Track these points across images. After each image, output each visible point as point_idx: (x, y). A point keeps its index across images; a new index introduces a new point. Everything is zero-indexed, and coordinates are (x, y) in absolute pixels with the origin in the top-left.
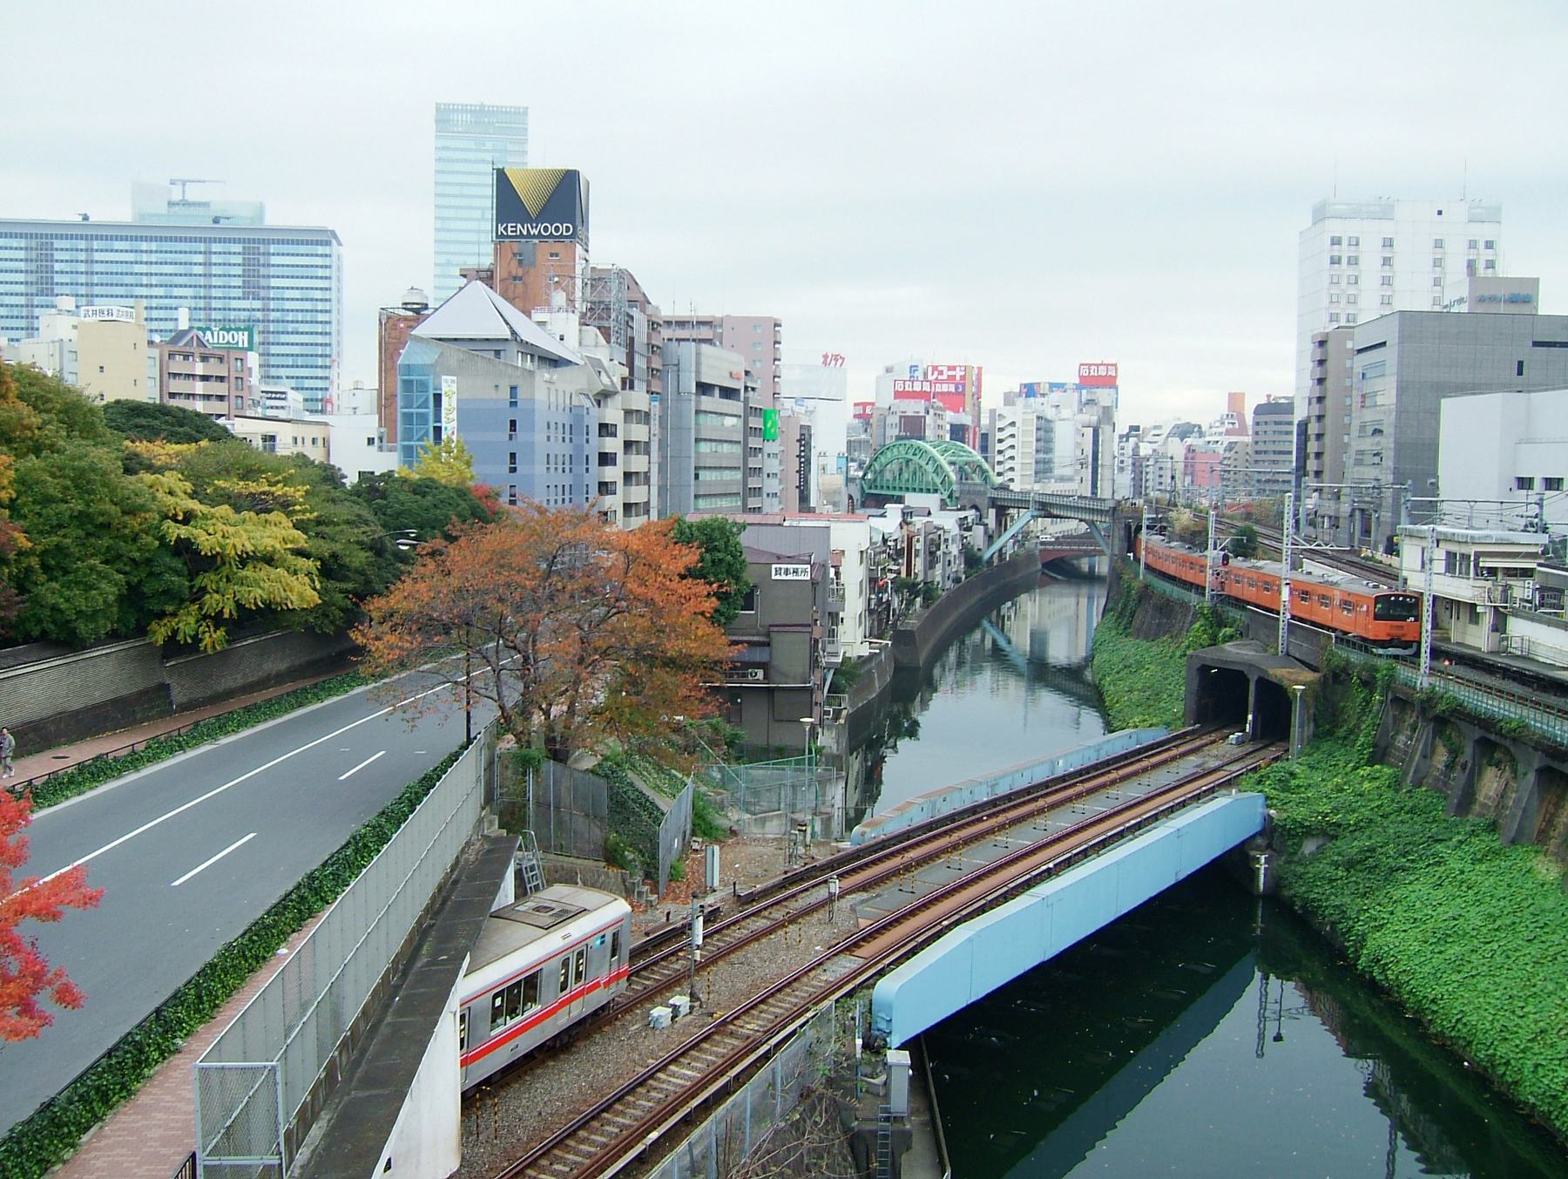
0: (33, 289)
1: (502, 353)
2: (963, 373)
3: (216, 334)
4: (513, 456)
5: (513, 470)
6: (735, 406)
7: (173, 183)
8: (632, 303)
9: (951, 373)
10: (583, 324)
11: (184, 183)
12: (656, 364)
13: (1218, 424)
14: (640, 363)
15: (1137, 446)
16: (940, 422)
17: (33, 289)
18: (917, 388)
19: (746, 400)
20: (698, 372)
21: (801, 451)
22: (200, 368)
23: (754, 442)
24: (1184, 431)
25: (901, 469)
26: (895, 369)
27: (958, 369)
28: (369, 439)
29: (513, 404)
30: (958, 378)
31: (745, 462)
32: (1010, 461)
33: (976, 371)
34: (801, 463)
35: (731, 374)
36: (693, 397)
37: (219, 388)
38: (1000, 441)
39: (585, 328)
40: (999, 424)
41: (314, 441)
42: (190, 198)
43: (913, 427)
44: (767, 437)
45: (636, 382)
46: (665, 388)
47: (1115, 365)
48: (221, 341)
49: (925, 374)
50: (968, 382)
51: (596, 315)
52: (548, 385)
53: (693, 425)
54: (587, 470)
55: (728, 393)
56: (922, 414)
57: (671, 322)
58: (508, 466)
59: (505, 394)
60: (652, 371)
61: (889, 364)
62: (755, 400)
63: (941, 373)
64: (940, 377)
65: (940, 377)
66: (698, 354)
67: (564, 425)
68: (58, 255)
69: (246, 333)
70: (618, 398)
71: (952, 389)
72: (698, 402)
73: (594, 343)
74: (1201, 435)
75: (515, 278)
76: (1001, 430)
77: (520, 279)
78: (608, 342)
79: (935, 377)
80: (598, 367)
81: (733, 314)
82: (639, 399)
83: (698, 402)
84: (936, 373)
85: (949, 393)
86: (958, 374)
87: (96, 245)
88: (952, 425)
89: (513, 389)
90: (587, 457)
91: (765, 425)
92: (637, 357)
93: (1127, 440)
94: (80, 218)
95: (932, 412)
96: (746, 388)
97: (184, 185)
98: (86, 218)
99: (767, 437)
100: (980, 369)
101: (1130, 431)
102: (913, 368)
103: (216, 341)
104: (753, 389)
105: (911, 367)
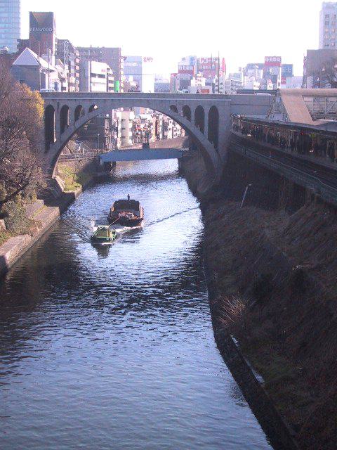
6: (104, 80)
43: (185, 84)
55: (101, 76)
62: (111, 79)
95: (194, 78)
100: (223, 59)
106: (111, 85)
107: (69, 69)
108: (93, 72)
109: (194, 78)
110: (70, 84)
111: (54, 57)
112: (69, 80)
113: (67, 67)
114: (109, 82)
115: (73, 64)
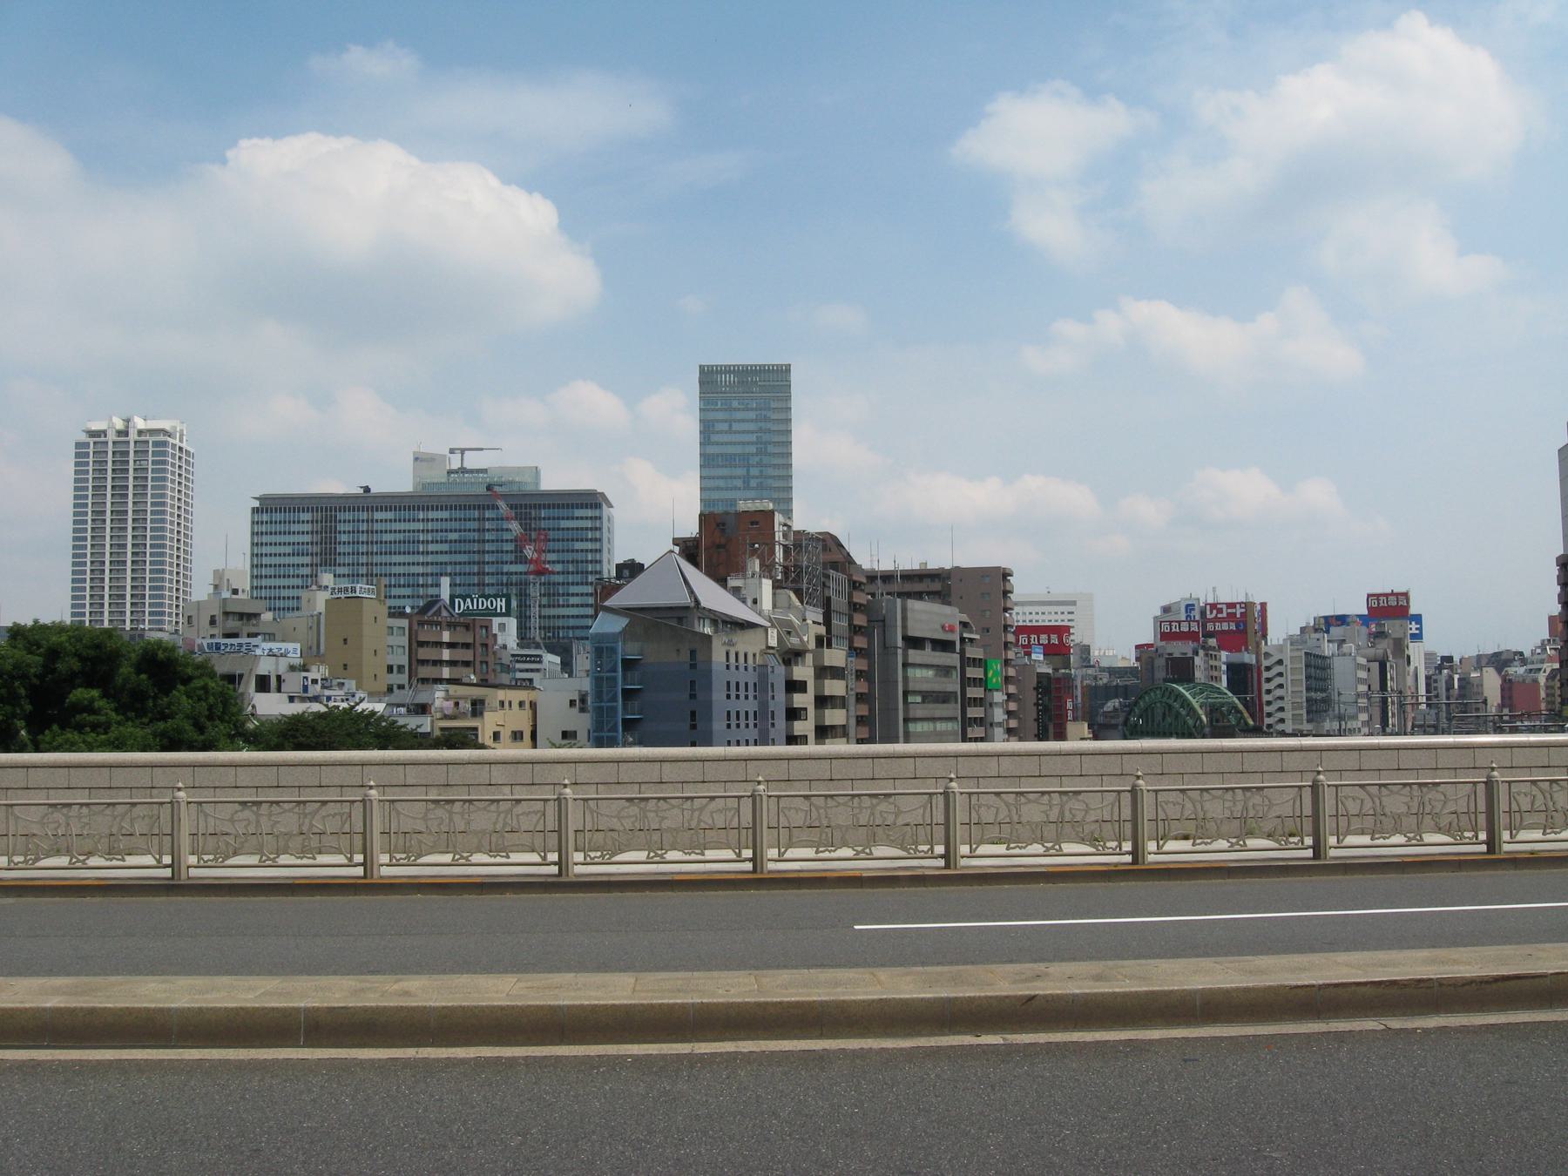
0: (317, 560)
1: (685, 620)
2: (1243, 610)
3: (475, 600)
4: (693, 714)
5: (694, 727)
6: (953, 659)
7: (452, 451)
8: (835, 565)
9: (1229, 611)
10: (777, 586)
11: (463, 451)
12: (860, 620)
13: (1539, 651)
14: (839, 624)
15: (1451, 678)
16: (1212, 663)
17: (317, 560)
18: (1185, 628)
19: (962, 653)
20: (904, 627)
21: (1038, 699)
22: (446, 637)
23: (974, 692)
24: (1499, 661)
25: (1164, 714)
26: (1173, 609)
27: (1238, 606)
28: (571, 701)
29: (693, 666)
30: (1238, 616)
31: (964, 712)
32: (1279, 701)
33: (1259, 608)
34: (1038, 711)
35: (943, 627)
36: (900, 651)
37: (467, 655)
38: (1268, 680)
39: (778, 591)
40: (1265, 663)
41: (521, 704)
42: (468, 465)
44: (989, 687)
45: (834, 640)
46: (871, 643)
47: (1406, 595)
48: (480, 607)
49: (1203, 613)
50: (1249, 620)
51: (791, 580)
52: (727, 648)
53: (900, 679)
54: (773, 725)
55: (943, 646)
56: (1190, 655)
57: (876, 577)
58: (689, 722)
59: (685, 657)
60: (855, 630)
61: (1165, 603)
62: (973, 652)
63: (1220, 611)
64: (1219, 616)
65: (1219, 616)
66: (904, 610)
67: (746, 684)
68: (341, 527)
69: (504, 600)
70: (809, 658)
71: (1233, 627)
72: (905, 656)
73: (787, 606)
74: (1524, 661)
75: (719, 546)
76: (1268, 669)
77: (723, 546)
78: (802, 602)
79: (1213, 615)
80: (787, 629)
81: (964, 565)
82: (836, 656)
83: (905, 656)
84: (1215, 612)
85: (1229, 631)
86: (1239, 611)
87: (378, 515)
88: (1230, 666)
89: (693, 653)
90: (773, 712)
91: (986, 674)
92: (834, 616)
93: (1440, 673)
94: (362, 491)
95: (1201, 652)
96: (962, 640)
97: (462, 454)
98: (367, 490)
99: (989, 687)
100: (1263, 605)
101: (1442, 663)
102: (1189, 608)
103: (475, 608)
104: (971, 640)
105: (1187, 606)
106: (973, 672)
107: (827, 622)
108: (910, 633)
109: (1201, 652)
110: (823, 672)
111: (767, 584)
112: (818, 658)
113: (815, 615)
114: (966, 662)
115: (840, 602)
